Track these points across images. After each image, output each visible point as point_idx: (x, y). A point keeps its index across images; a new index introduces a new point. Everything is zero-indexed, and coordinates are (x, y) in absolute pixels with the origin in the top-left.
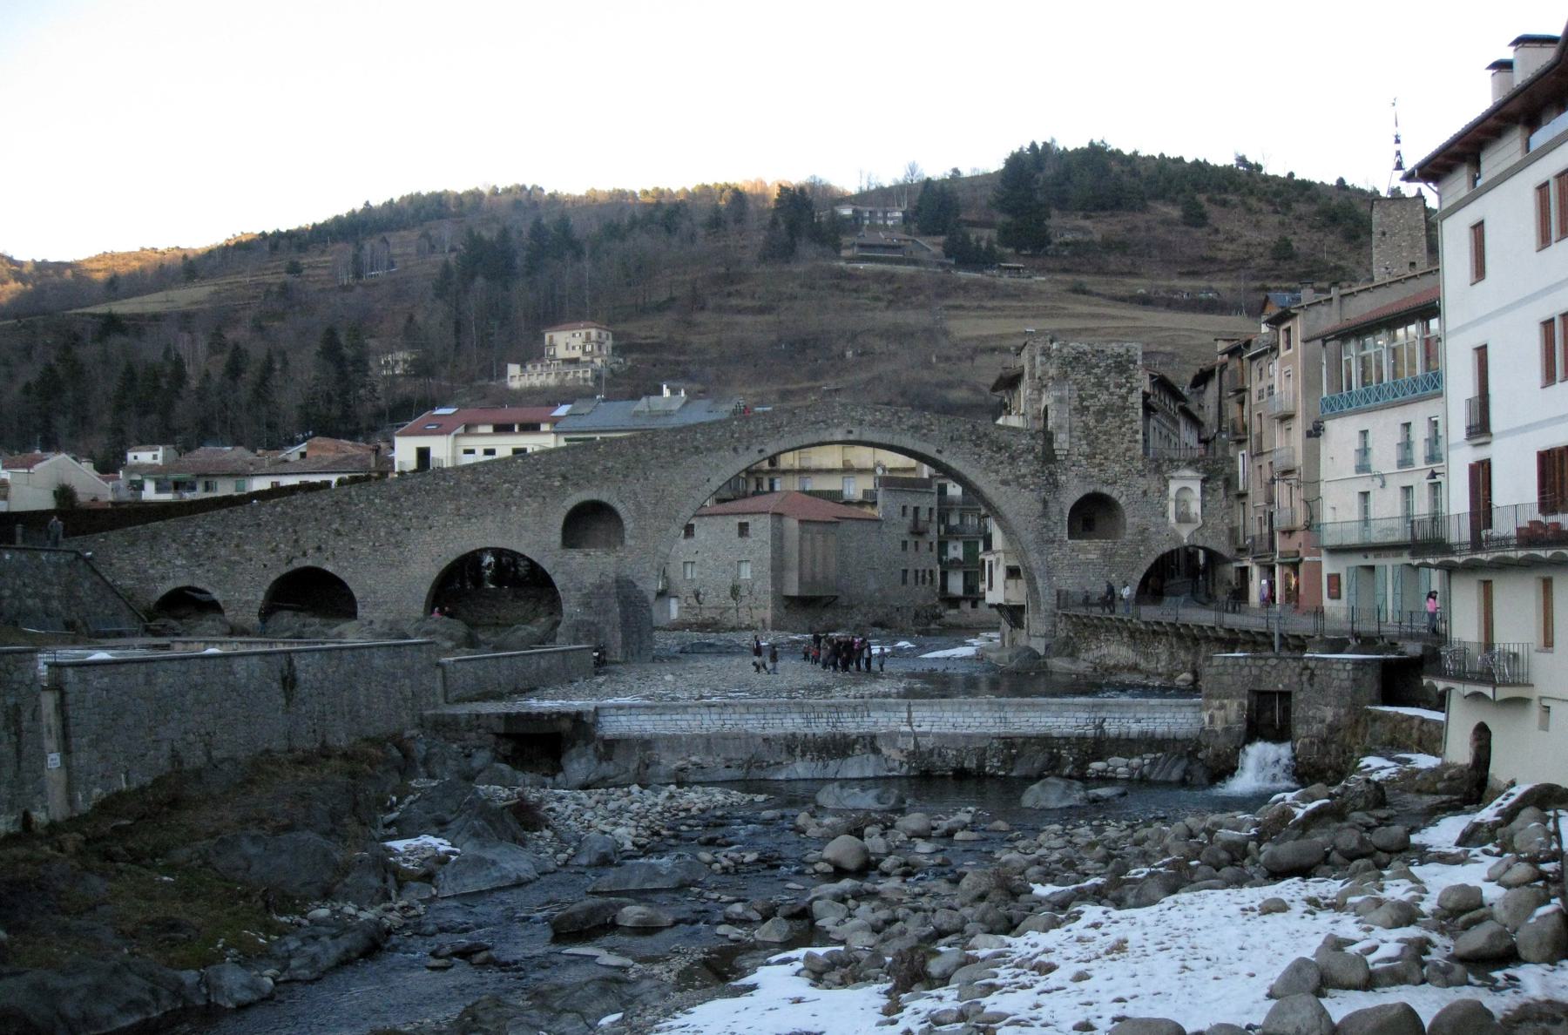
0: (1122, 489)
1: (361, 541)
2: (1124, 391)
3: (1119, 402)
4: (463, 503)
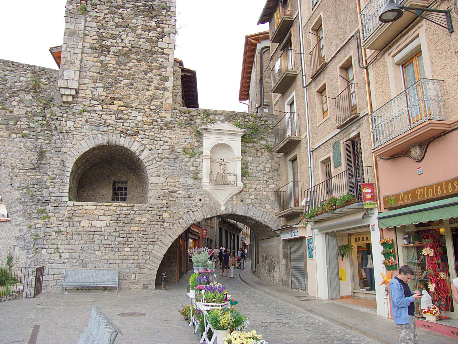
0: (145, 142)
2: (153, 34)
3: (148, 46)
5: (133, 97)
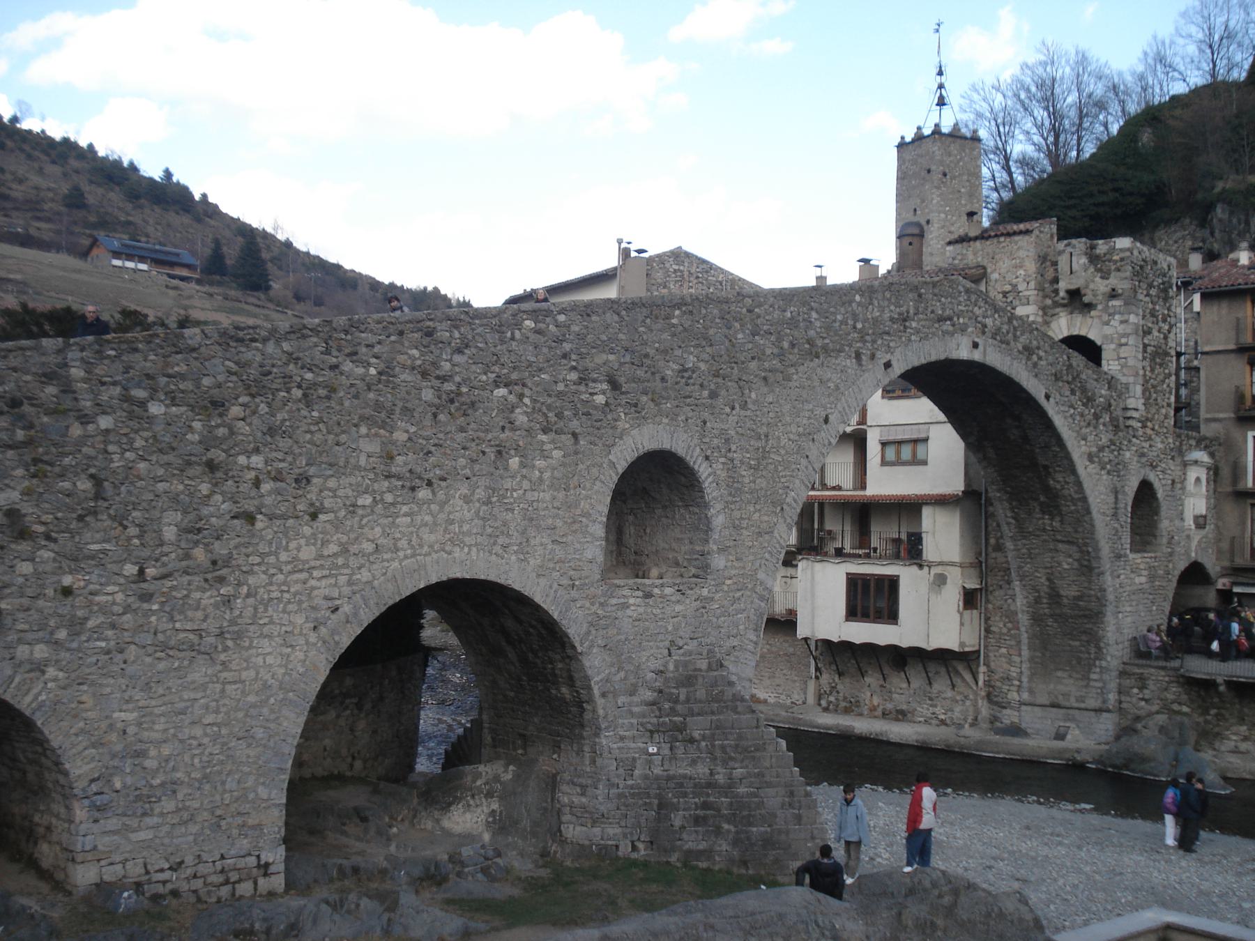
1: (98, 559)
4: (400, 436)
5: (1156, 416)
